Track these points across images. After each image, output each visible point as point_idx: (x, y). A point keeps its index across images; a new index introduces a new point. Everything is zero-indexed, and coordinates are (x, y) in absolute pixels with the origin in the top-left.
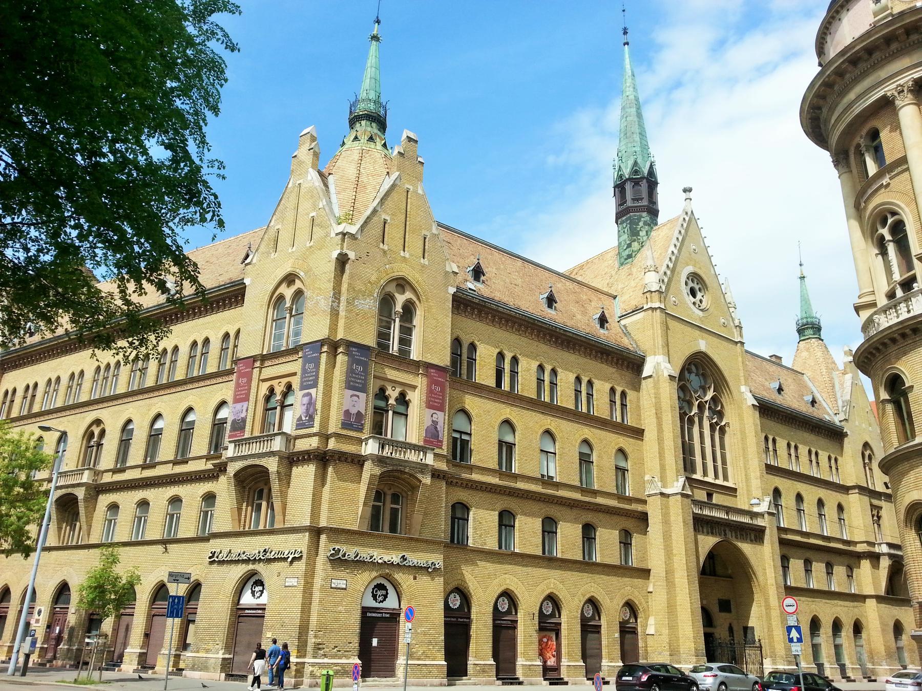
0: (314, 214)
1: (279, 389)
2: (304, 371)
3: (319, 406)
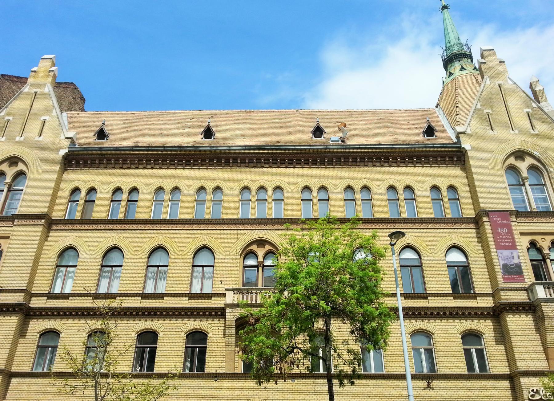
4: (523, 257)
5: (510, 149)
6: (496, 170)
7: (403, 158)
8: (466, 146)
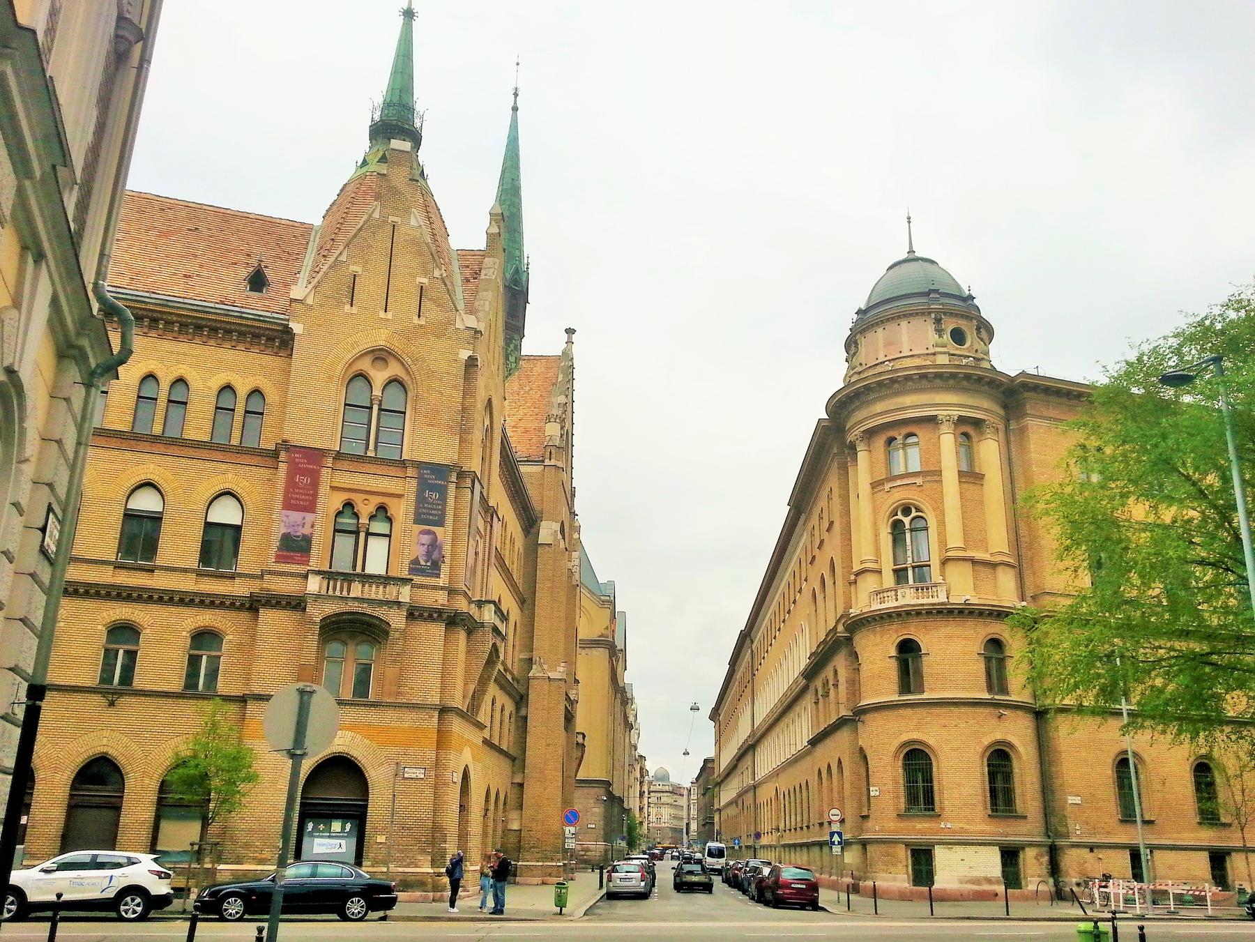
0: (425, 281)
1: (365, 509)
2: (420, 500)
3: (447, 550)
4: (319, 525)
5: (366, 343)
6: (330, 378)
7: (183, 325)
8: (297, 328)
